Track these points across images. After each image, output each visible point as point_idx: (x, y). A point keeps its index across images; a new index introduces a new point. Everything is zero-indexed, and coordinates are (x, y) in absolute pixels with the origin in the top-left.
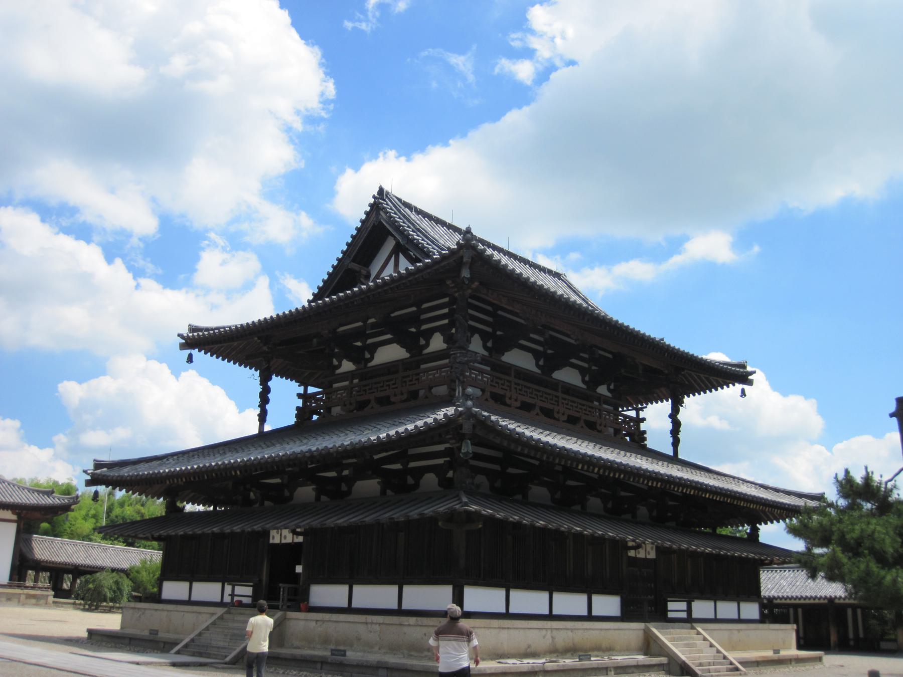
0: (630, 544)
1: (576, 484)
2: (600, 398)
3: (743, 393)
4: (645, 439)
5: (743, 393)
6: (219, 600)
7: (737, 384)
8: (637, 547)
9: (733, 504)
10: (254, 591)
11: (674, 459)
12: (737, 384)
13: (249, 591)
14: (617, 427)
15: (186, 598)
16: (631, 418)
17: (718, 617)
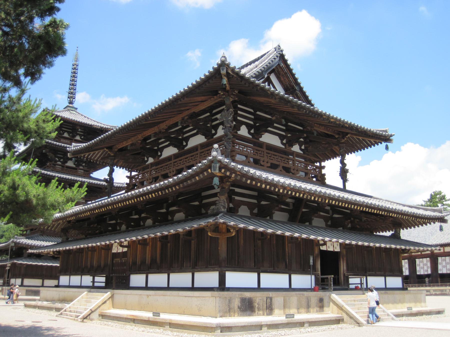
0: (321, 242)
1: (303, 210)
2: (293, 153)
3: (387, 148)
4: (325, 179)
5: (387, 148)
6: (80, 285)
7: (383, 143)
8: (325, 243)
9: (379, 214)
10: (106, 280)
11: (344, 190)
12: (383, 143)
13: (103, 279)
14: (306, 171)
15: (68, 284)
16: (317, 167)
17: (170, 286)
